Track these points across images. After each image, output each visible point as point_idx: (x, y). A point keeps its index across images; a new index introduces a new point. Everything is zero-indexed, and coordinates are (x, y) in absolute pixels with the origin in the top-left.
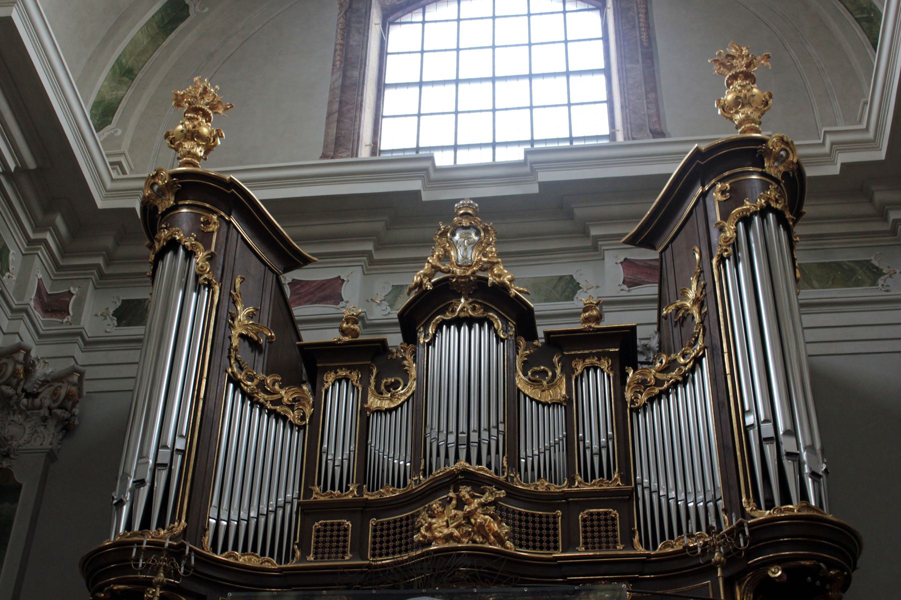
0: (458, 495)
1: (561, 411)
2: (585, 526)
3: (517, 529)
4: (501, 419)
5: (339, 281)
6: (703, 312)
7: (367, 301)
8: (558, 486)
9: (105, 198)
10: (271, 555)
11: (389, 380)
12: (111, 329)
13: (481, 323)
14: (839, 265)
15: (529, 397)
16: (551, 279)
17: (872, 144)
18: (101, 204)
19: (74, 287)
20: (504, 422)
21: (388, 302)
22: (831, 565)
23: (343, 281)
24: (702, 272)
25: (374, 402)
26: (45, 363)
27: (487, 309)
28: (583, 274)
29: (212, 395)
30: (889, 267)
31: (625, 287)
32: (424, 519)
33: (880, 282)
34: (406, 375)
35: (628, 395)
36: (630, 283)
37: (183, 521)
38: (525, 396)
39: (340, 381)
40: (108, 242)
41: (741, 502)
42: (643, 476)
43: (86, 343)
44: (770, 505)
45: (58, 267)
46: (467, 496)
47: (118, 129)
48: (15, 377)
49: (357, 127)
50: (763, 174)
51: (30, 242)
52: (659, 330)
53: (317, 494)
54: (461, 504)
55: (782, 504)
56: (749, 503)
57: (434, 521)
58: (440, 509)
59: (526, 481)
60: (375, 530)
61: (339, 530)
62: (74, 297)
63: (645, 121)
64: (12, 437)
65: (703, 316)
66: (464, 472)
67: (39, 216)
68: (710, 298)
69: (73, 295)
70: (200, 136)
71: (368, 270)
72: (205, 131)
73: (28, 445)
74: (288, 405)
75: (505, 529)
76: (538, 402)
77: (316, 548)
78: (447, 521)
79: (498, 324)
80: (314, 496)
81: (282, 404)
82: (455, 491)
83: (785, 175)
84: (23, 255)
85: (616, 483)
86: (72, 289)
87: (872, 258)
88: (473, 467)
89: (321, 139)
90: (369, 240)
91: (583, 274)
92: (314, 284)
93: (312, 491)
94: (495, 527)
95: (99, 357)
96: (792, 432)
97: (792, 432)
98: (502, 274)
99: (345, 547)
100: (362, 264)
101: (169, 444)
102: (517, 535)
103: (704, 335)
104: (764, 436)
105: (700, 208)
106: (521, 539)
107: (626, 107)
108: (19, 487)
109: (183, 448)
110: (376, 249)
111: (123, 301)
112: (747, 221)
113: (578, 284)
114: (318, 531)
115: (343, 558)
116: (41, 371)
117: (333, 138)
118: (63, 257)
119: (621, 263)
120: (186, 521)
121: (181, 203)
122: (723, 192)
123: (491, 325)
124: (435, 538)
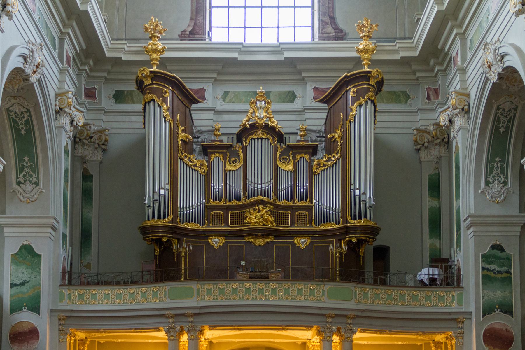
0: (259, 208)
3: (276, 218)
4: (272, 178)
5: (203, 90)
6: (342, 142)
7: (214, 98)
8: (289, 202)
11: (233, 159)
14: (395, 92)
16: (286, 92)
20: (273, 179)
21: (223, 99)
22: (370, 238)
23: (205, 90)
24: (343, 125)
25: (228, 167)
28: (298, 91)
30: (413, 95)
31: (314, 101)
32: (247, 214)
33: (409, 101)
34: (239, 157)
35: (314, 169)
37: (172, 215)
38: (280, 168)
40: (110, 67)
43: (105, 112)
44: (355, 219)
45: (88, 76)
49: (205, 3)
53: (211, 202)
55: (359, 219)
56: (349, 217)
57: (251, 216)
59: (279, 201)
61: (219, 215)
62: (97, 90)
63: (327, 10)
65: (341, 145)
67: (83, 60)
68: (344, 137)
69: (96, 89)
71: (214, 83)
73: (92, 158)
74: (199, 167)
75: (273, 219)
76: (284, 170)
81: (197, 166)
82: (258, 206)
85: (307, 203)
86: (95, 86)
87: (407, 90)
89: (189, 8)
90: (215, 72)
91: (298, 92)
92: (194, 91)
93: (209, 200)
94: (270, 218)
95: (111, 118)
97: (365, 193)
100: (212, 82)
102: (276, 220)
103: (341, 151)
105: (345, 97)
106: (277, 221)
107: (320, 2)
109: (168, 188)
110: (217, 75)
111: (116, 91)
113: (296, 95)
115: (221, 225)
117: (195, 8)
119: (313, 89)
124: (251, 222)
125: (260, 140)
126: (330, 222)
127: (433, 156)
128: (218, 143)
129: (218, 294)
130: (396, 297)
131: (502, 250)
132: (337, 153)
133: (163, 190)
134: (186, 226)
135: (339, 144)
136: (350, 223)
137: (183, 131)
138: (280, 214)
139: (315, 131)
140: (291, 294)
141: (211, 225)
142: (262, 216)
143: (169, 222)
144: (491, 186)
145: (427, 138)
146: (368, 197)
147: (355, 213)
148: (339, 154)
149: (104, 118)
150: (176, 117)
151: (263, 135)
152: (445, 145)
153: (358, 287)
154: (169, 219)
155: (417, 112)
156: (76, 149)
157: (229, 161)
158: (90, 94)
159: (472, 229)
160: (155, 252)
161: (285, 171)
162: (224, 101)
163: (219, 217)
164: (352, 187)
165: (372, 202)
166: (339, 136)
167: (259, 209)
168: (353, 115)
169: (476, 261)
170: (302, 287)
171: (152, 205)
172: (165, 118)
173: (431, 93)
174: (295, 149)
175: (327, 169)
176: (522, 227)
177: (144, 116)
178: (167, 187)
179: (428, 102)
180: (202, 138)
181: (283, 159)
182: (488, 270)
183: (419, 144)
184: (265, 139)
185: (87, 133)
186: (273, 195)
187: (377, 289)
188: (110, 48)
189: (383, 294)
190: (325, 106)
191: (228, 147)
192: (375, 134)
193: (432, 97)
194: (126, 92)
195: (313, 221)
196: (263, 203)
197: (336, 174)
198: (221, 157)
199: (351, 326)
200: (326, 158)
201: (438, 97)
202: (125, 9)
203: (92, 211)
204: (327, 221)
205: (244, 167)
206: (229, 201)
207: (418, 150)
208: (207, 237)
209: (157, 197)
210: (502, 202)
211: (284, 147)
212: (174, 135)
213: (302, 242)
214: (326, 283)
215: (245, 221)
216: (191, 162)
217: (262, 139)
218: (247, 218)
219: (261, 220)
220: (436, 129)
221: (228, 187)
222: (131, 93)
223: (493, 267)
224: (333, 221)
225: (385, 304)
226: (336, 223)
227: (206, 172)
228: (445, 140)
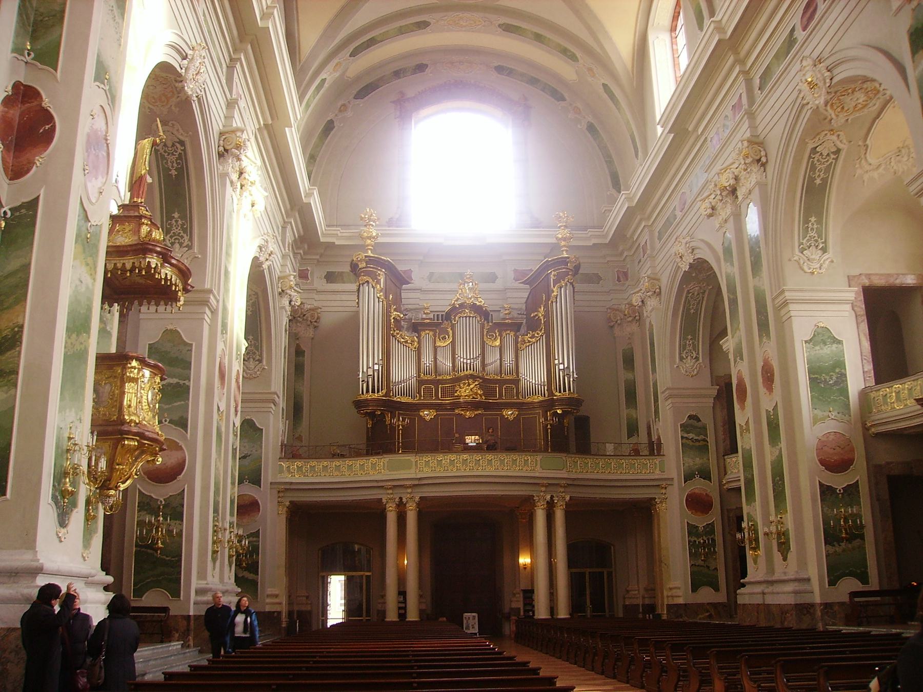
9: (322, 237)
11: (443, 336)
17: (605, 236)
18: (322, 240)
22: (574, 409)
25: (438, 344)
44: (560, 392)
45: (302, 258)
52: (526, 302)
54: (469, 385)
66: (471, 375)
95: (322, 297)
97: (568, 367)
98: (480, 302)
122: (554, 275)
125: (468, 318)
128: (428, 321)
129: (436, 466)
131: (699, 420)
132: (541, 331)
133: (377, 366)
134: (399, 400)
135: (543, 322)
136: (556, 396)
137: (395, 310)
139: (516, 309)
141: (422, 398)
143: (383, 396)
144: (684, 360)
146: (571, 371)
147: (560, 385)
148: (543, 332)
149: (316, 297)
150: (389, 297)
151: (471, 313)
153: (569, 457)
154: (382, 393)
157: (439, 338)
159: (670, 401)
160: (367, 424)
162: (430, 281)
164: (556, 362)
165: (575, 376)
166: (542, 315)
167: (468, 383)
168: (554, 295)
169: (676, 431)
171: (366, 380)
172: (378, 298)
174: (502, 327)
175: (531, 345)
176: (714, 398)
177: (358, 296)
178: (381, 362)
180: (409, 315)
181: (490, 336)
182: (687, 438)
184: (473, 317)
185: (302, 313)
187: (586, 459)
190: (528, 286)
191: (438, 325)
196: (472, 377)
197: (540, 349)
198: (431, 333)
199: (564, 494)
201: (627, 279)
203: (303, 384)
205: (453, 343)
206: (440, 375)
207: (612, 327)
208: (419, 410)
209: (370, 372)
210: (695, 375)
211: (490, 324)
212: (387, 314)
213: (509, 413)
214: (538, 454)
215: (456, 394)
216: (403, 338)
217: (470, 317)
219: (471, 393)
220: (629, 308)
221: (438, 362)
222: (341, 274)
223: (691, 436)
225: (593, 472)
226: (541, 395)
227: (417, 347)
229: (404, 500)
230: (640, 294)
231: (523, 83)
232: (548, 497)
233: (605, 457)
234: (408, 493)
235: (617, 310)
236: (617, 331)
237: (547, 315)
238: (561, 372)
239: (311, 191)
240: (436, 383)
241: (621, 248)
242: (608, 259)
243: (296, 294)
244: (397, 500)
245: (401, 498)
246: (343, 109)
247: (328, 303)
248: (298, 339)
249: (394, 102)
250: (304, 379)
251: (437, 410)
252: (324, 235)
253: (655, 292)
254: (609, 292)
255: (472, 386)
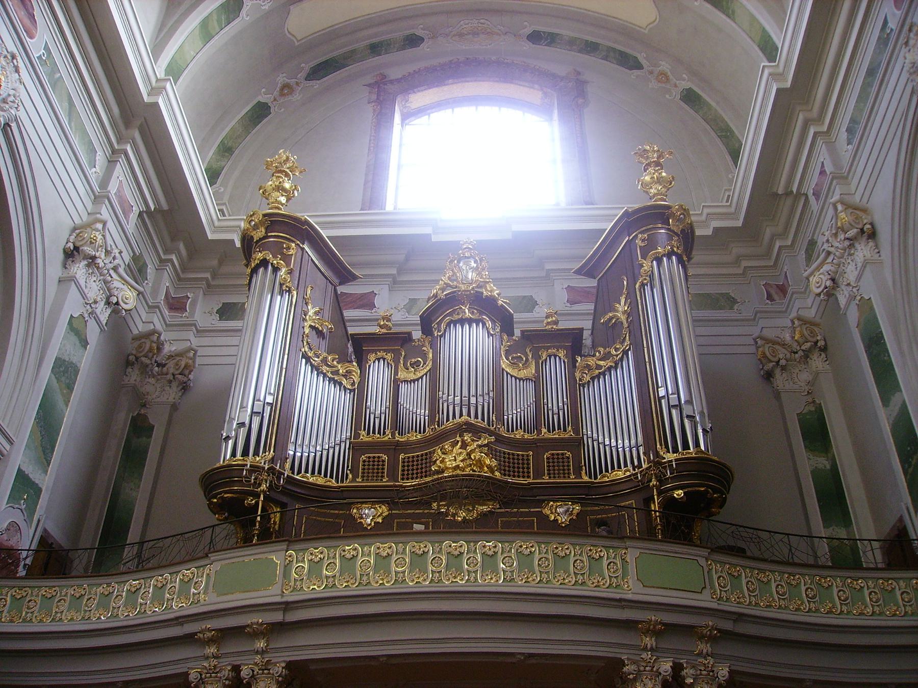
1: (531, 387)
2: (548, 462)
5: (373, 294)
8: (530, 435)
9: (213, 232)
10: (331, 477)
12: (215, 322)
13: (477, 322)
15: (510, 374)
18: (210, 236)
19: (190, 293)
22: (715, 490)
23: (376, 294)
24: (628, 293)
25: (402, 375)
26: (171, 343)
27: (481, 313)
29: (291, 366)
31: (568, 305)
33: (736, 307)
34: (424, 356)
35: (578, 375)
36: (572, 302)
37: (272, 451)
38: (507, 373)
39: (379, 360)
40: (215, 263)
41: (656, 448)
42: (588, 431)
44: (675, 450)
45: (180, 279)
46: (469, 440)
47: (221, 188)
48: (151, 352)
50: (669, 230)
51: (161, 261)
52: (592, 333)
58: (450, 448)
59: (508, 431)
60: (403, 462)
61: (378, 461)
62: (190, 299)
64: (148, 393)
65: (630, 324)
66: (467, 423)
69: (189, 298)
70: (284, 190)
72: (287, 185)
75: (494, 463)
76: (516, 378)
77: (363, 473)
78: (455, 457)
79: (489, 324)
80: (361, 437)
83: (683, 231)
84: (156, 269)
85: (570, 433)
86: (189, 294)
88: (472, 420)
94: (488, 462)
95: (205, 341)
96: (689, 402)
98: (492, 290)
99: (383, 473)
101: (262, 399)
103: (629, 336)
104: (671, 404)
106: (505, 470)
108: (154, 426)
109: (272, 402)
112: (659, 260)
113: (536, 301)
114: (364, 461)
115: (381, 480)
116: (168, 349)
118: (183, 272)
120: (274, 452)
121: (269, 234)
122: (643, 241)
123: (484, 324)
124: (447, 468)
126: (619, 467)
127: (799, 383)
130: (811, 594)
138: (511, 456)
140: (537, 568)
142: (469, 454)
145: (782, 353)
148: (627, 342)
152: (821, 355)
155: (754, 319)
156: (127, 375)
158: (177, 305)
161: (517, 380)
163: (378, 465)
164: (662, 392)
167: (463, 441)
170: (568, 552)
173: (773, 292)
179: (770, 303)
183: (771, 361)
186: (494, 418)
187: (762, 571)
188: (217, 227)
189: (778, 583)
192: (692, 317)
193: (776, 297)
194: (240, 304)
195: (584, 471)
200: (600, 353)
202: (259, 203)
204: (613, 468)
208: (349, 506)
218: (438, 462)
220: (800, 325)
224: (626, 465)
225: (786, 608)
228: (819, 344)
229: (245, 673)
230: (826, 268)
231: (573, 53)
232: (666, 667)
233: (814, 571)
234: (257, 652)
235: (774, 343)
236: (780, 379)
237: (633, 312)
238: (674, 412)
239: (161, 84)
240: (395, 448)
241: (768, 232)
242: (745, 263)
243: (125, 287)
244: (225, 673)
245: (236, 669)
246: (287, 90)
247: (216, 351)
248: (144, 405)
249: (369, 85)
250: (141, 475)
251: (392, 504)
252: (216, 229)
253: (862, 230)
254: (754, 319)
255: (469, 449)
